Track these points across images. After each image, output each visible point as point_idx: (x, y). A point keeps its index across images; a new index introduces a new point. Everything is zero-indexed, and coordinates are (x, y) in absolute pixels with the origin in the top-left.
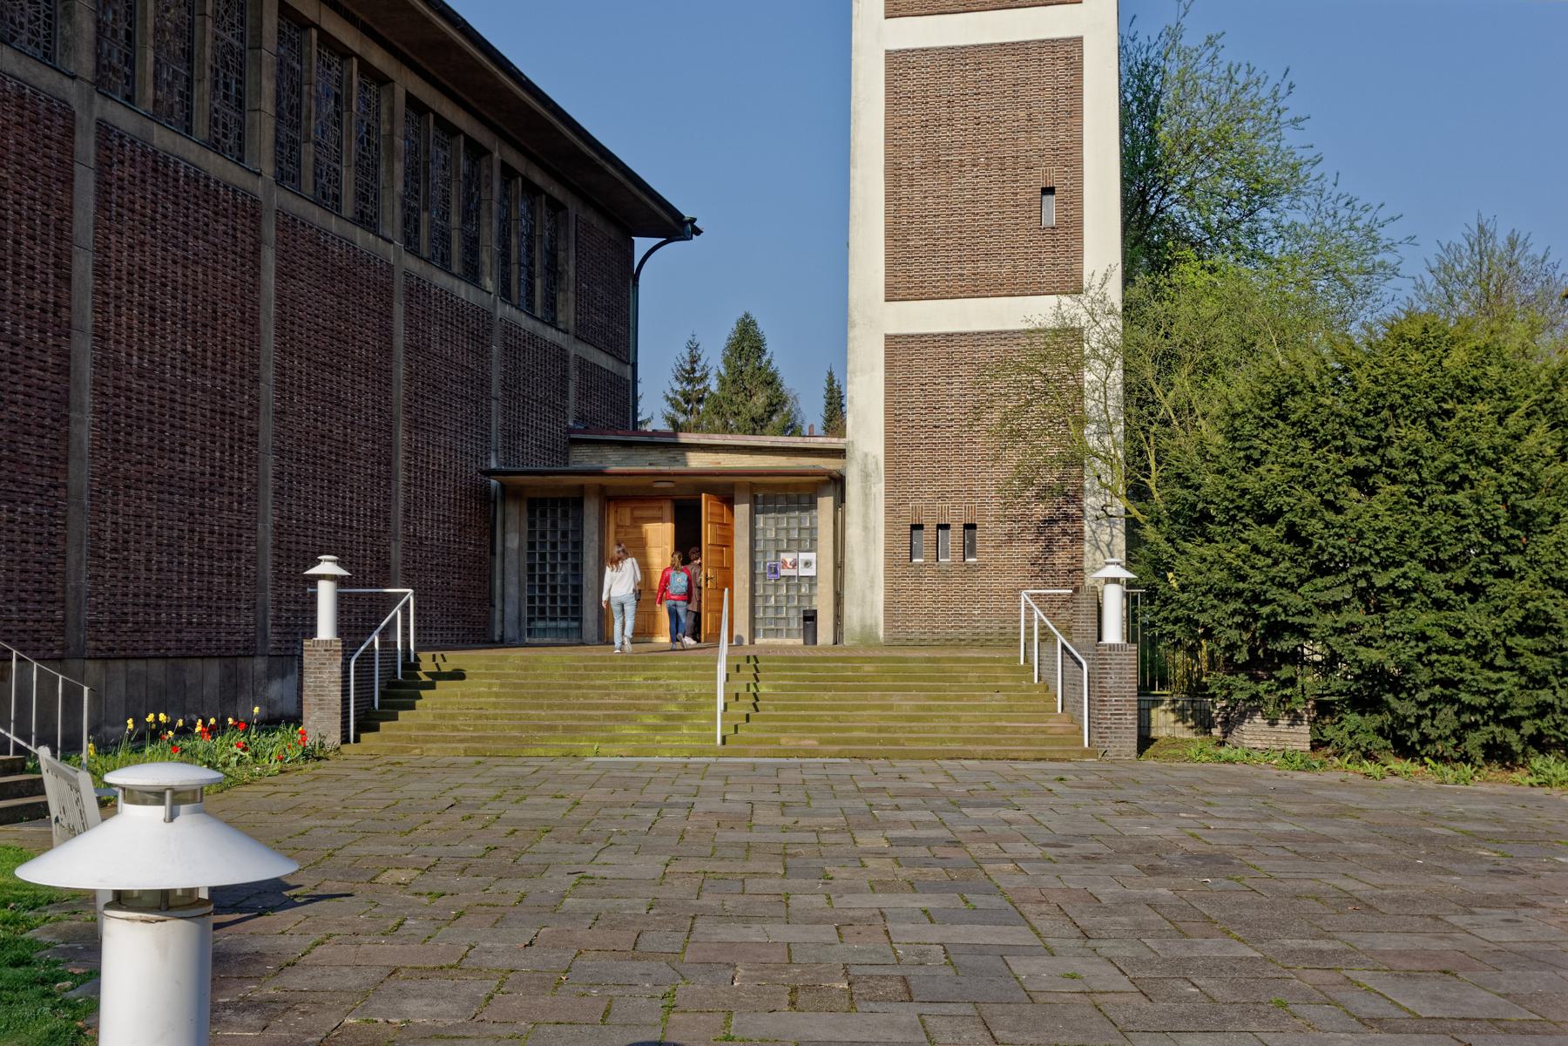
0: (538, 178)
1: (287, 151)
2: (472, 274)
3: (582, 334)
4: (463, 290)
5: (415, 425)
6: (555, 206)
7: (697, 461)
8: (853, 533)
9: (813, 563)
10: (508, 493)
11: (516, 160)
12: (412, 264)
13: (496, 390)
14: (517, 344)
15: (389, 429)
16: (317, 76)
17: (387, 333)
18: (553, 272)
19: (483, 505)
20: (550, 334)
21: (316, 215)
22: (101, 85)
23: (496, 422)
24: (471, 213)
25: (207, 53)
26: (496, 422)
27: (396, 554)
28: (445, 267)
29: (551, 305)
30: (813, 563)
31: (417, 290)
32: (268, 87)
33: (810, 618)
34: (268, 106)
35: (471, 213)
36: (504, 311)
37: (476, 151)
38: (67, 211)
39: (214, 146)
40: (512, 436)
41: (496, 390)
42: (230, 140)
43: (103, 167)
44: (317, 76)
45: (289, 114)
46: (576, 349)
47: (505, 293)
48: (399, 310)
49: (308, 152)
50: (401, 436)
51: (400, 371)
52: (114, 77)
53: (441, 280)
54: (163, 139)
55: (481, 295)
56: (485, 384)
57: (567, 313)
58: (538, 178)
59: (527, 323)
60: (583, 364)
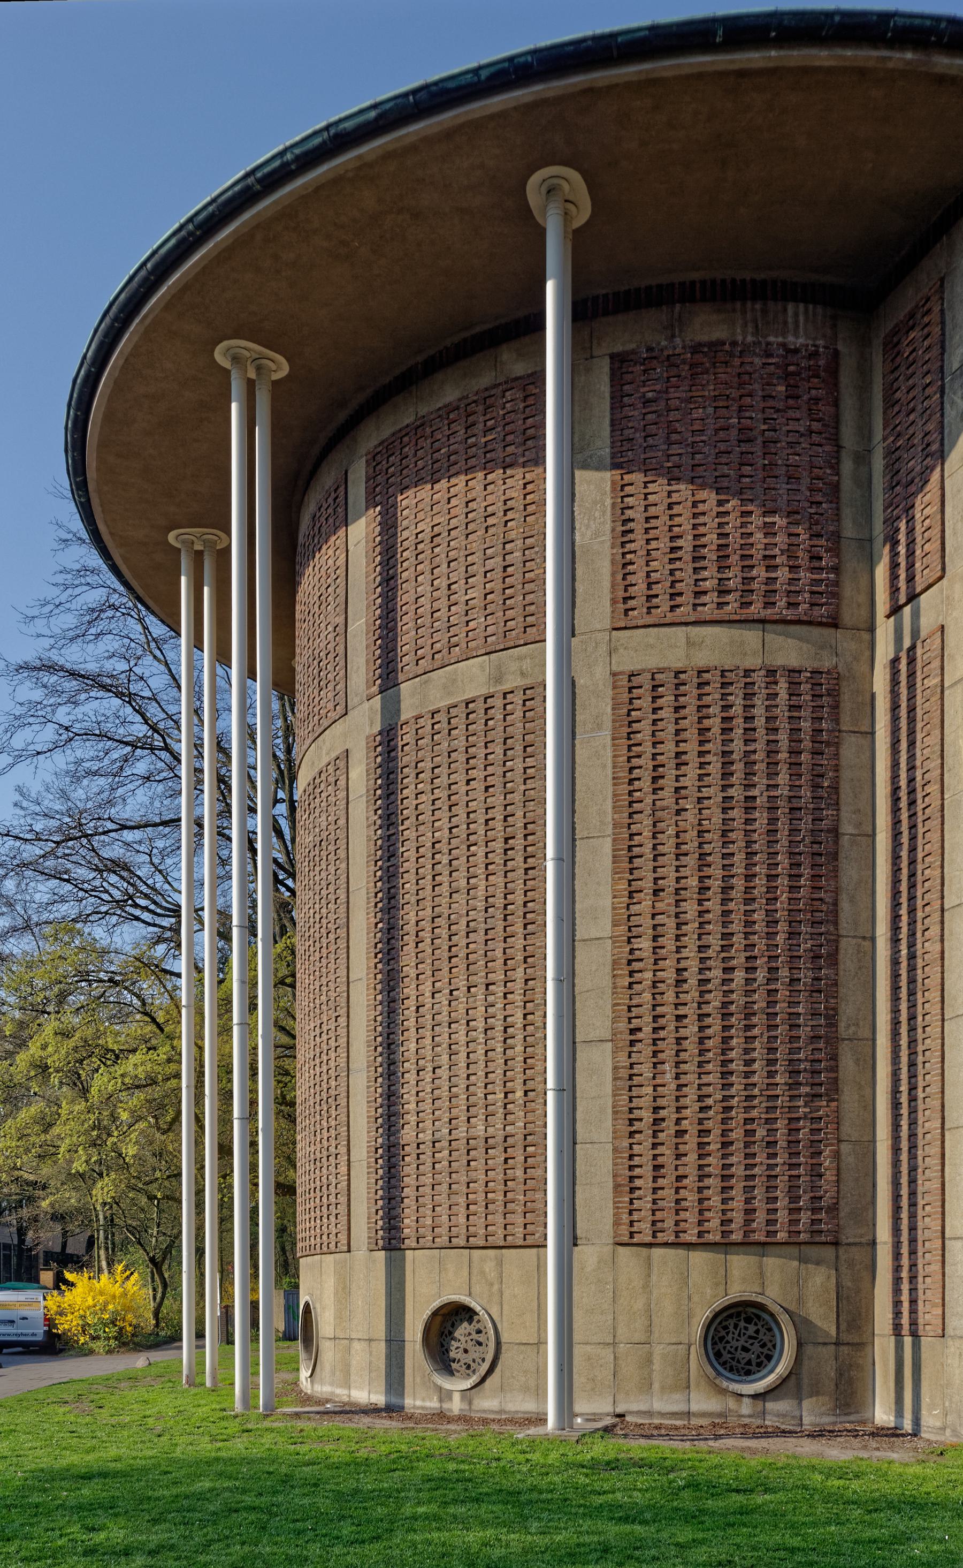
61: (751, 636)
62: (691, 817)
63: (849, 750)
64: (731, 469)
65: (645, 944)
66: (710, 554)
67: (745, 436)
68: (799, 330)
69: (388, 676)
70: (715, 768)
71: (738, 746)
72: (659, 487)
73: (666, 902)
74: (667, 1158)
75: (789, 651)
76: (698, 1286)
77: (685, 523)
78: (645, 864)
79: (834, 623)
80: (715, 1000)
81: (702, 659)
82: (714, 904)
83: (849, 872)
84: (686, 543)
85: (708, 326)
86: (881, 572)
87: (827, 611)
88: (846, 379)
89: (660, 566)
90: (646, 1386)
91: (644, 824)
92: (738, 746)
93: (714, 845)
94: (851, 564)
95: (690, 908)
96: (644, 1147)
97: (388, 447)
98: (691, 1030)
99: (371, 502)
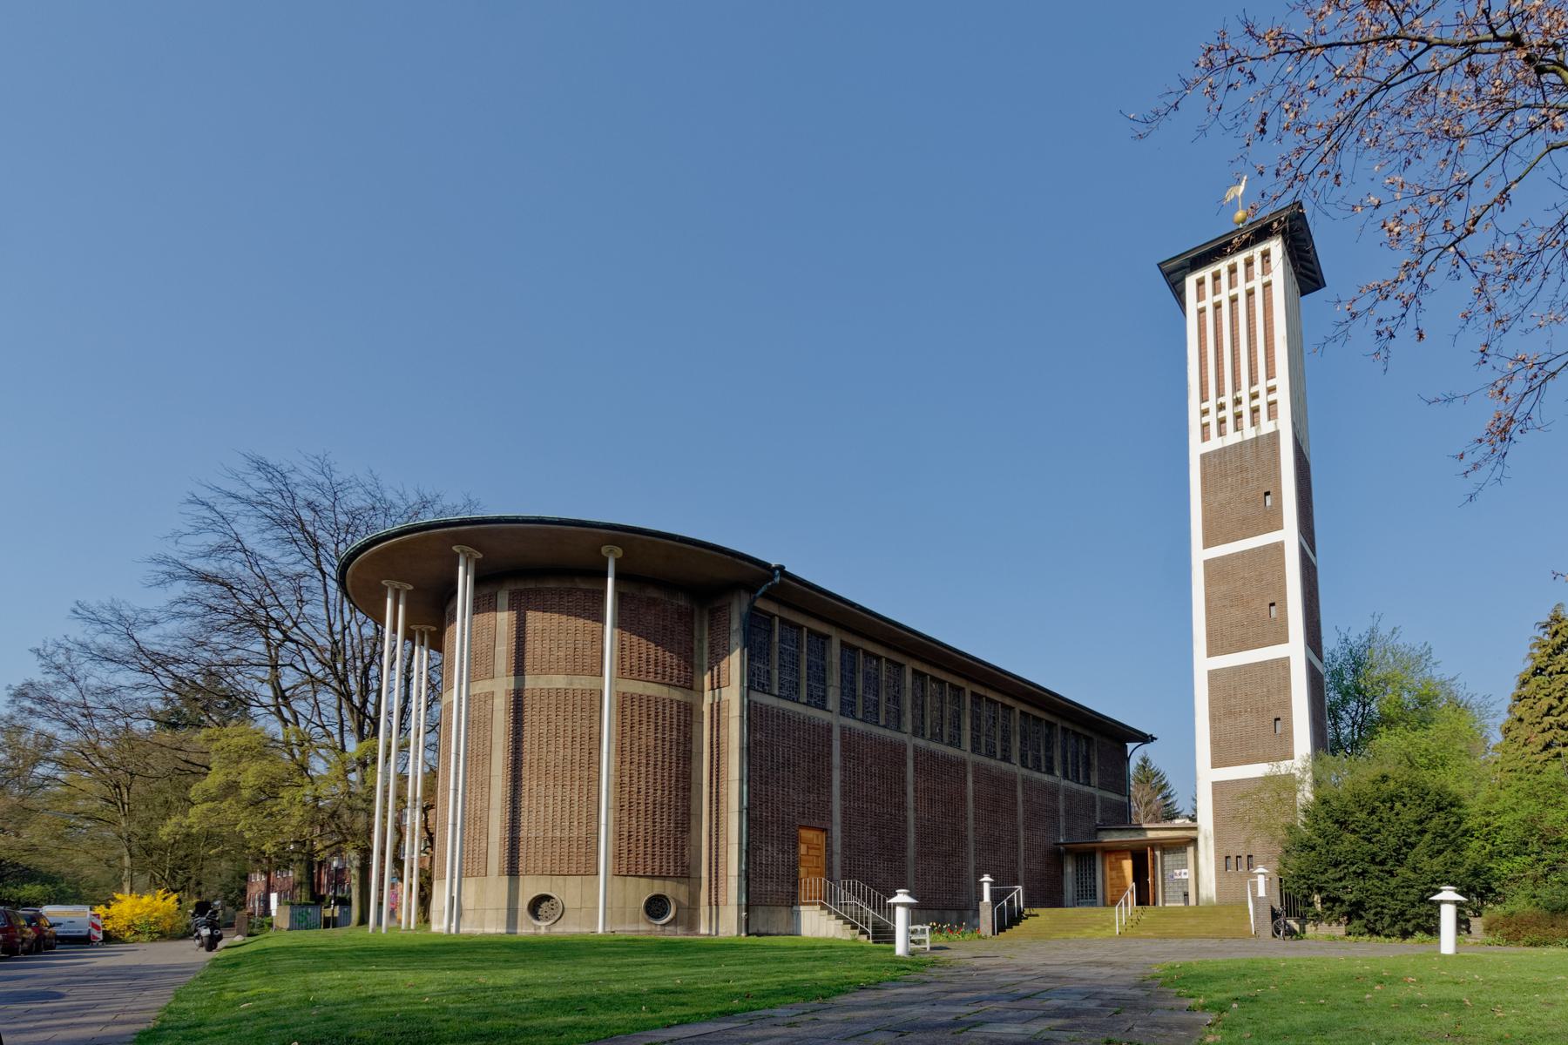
0: (1078, 730)
1: (975, 742)
2: (1050, 771)
3: (1102, 787)
4: (1046, 778)
5: (1027, 828)
6: (1089, 740)
7: (1151, 835)
8: (1202, 861)
9: (1186, 874)
10: (1068, 851)
11: (1067, 725)
12: (1025, 771)
13: (1062, 812)
14: (1070, 795)
15: (1017, 831)
16: (985, 712)
17: (1015, 797)
18: (1088, 765)
19: (1056, 857)
20: (1087, 789)
21: (986, 760)
22: (915, 734)
23: (1062, 824)
24: (1049, 748)
25: (947, 714)
26: (1062, 824)
27: (1021, 876)
28: (1039, 770)
29: (1087, 777)
30: (1186, 874)
31: (1026, 781)
32: (968, 721)
33: (1186, 895)
34: (968, 727)
35: (1049, 748)
36: (1065, 783)
37: (1050, 725)
38: (905, 773)
39: (951, 744)
40: (1069, 830)
41: (1062, 812)
42: (955, 742)
43: (915, 758)
44: (985, 712)
45: (976, 728)
46: (1098, 793)
47: (1065, 776)
48: (1019, 789)
49: (983, 740)
50: (1022, 833)
51: (1020, 810)
52: (918, 731)
53: (1037, 775)
54: (934, 746)
55: (1057, 779)
56: (1056, 811)
57: (1095, 779)
58: (1078, 730)
59: (1075, 786)
60: (1103, 800)
61: (665, 689)
62: (644, 741)
63: (695, 727)
64: (659, 638)
65: (627, 779)
66: (652, 661)
67: (665, 628)
68: (682, 602)
69: (519, 670)
70: (652, 726)
71: (660, 721)
72: (635, 638)
73: (635, 766)
74: (633, 846)
75: (677, 695)
76: (646, 889)
77: (644, 650)
78: (627, 754)
79: (691, 688)
80: (651, 799)
81: (648, 693)
82: (651, 769)
83: (695, 764)
84: (644, 656)
85: (653, 593)
86: (707, 678)
87: (690, 684)
88: (696, 618)
89: (635, 662)
90: (623, 922)
91: (627, 741)
92: (660, 721)
93: (652, 751)
94: (697, 673)
95: (643, 770)
96: (624, 844)
97: (521, 593)
98: (642, 807)
99: (511, 608)
